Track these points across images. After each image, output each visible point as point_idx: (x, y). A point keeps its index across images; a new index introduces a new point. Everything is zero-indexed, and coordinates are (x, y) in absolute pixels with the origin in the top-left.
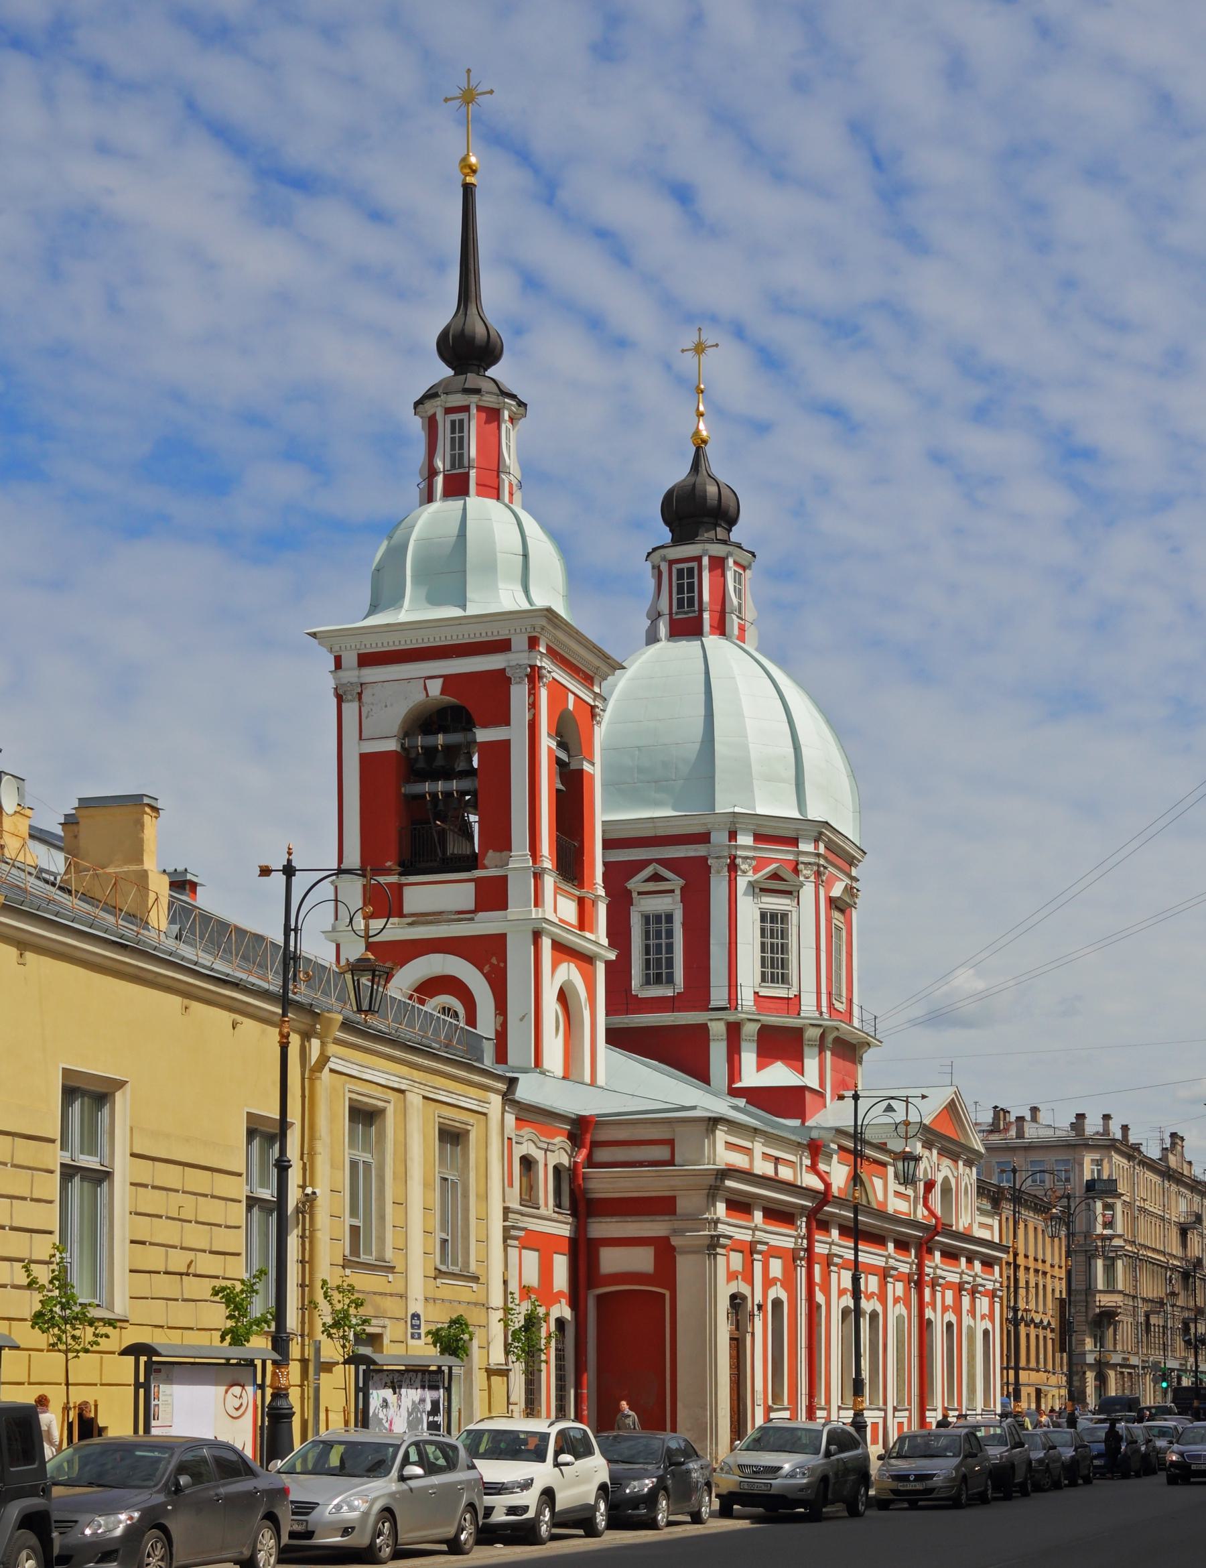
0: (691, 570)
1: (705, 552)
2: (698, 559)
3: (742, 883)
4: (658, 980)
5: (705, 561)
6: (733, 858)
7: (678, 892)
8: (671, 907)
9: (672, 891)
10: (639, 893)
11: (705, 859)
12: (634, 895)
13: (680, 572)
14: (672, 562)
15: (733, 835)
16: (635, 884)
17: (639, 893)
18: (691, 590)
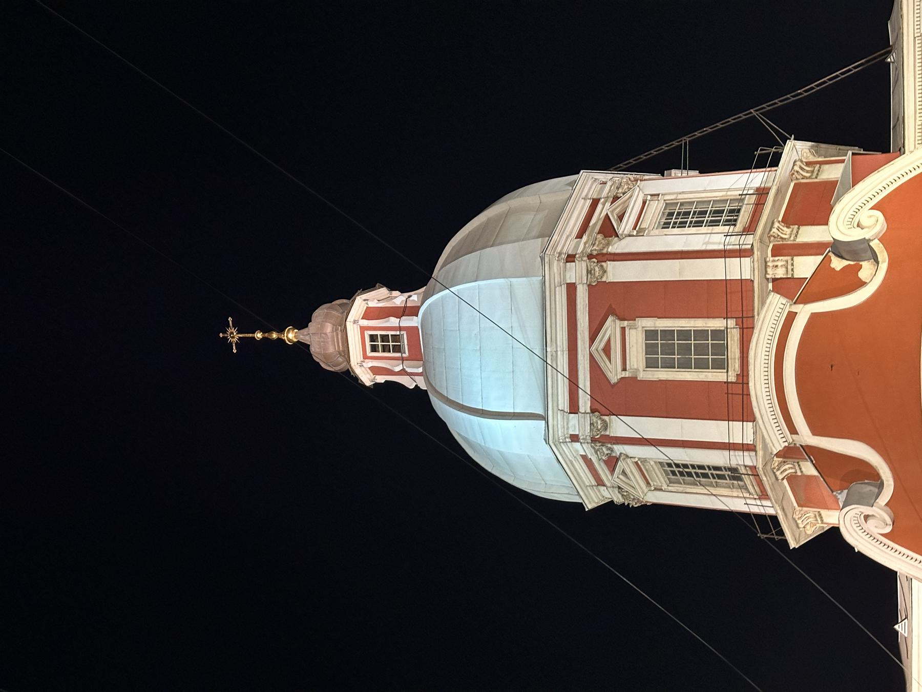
0: (373, 338)
1: (355, 322)
2: (363, 329)
3: (617, 247)
4: (721, 349)
5: (365, 323)
6: (590, 257)
7: (625, 323)
8: (640, 329)
9: (623, 329)
10: (624, 369)
11: (590, 286)
12: (624, 374)
13: (374, 349)
14: (365, 357)
15: (571, 258)
16: (614, 373)
17: (624, 369)
18: (384, 338)
